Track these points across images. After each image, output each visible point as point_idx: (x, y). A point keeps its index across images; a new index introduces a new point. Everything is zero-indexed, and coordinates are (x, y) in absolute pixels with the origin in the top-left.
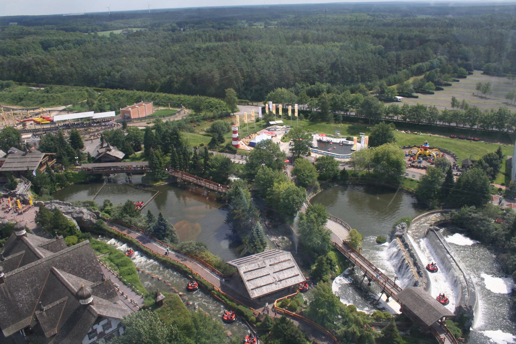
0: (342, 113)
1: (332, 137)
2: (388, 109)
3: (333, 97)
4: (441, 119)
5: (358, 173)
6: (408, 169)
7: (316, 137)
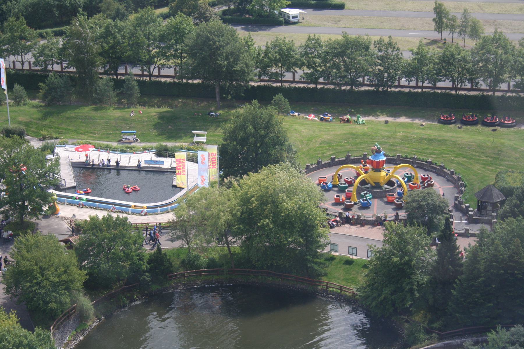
0: (137, 71)
1: (114, 150)
2: (266, 54)
3: (107, 28)
4: (411, 72)
5: (198, 257)
6: (336, 230)
7: (68, 154)
